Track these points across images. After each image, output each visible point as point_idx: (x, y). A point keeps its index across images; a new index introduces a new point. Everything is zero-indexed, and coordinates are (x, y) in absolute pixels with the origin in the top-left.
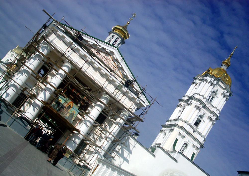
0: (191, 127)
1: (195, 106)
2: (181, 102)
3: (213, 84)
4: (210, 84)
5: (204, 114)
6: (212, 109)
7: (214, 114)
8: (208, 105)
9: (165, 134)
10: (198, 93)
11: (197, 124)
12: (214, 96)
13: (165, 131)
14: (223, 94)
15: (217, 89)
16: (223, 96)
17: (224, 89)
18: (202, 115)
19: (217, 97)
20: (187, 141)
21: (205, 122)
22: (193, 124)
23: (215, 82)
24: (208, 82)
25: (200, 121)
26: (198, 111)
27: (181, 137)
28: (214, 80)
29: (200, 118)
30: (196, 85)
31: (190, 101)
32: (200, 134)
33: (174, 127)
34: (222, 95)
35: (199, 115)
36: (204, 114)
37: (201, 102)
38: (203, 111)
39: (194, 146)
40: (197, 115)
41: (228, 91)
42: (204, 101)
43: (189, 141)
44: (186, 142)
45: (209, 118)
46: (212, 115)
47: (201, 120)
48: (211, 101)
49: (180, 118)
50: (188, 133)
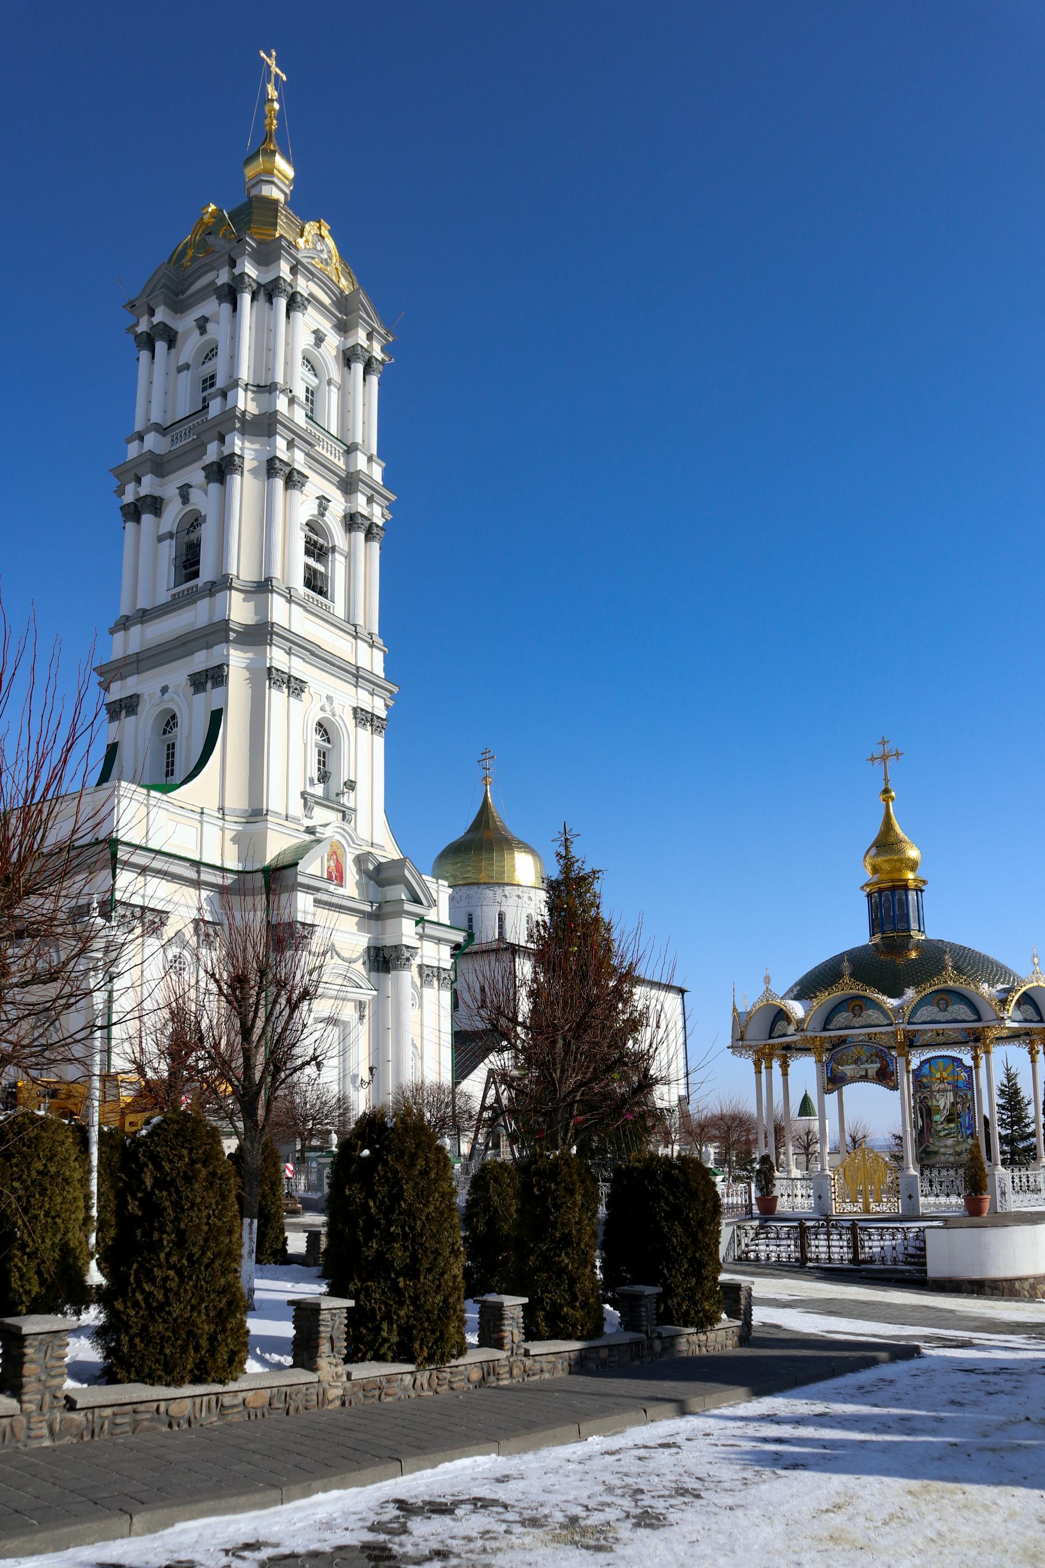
5: (323, 502)
12: (314, 381)
14: (348, 358)
17: (343, 328)
20: (324, 700)
30: (171, 343)
33: (208, 647)
36: (323, 502)
38: (317, 485)
44: (322, 715)
46: (361, 499)
50: (312, 653)
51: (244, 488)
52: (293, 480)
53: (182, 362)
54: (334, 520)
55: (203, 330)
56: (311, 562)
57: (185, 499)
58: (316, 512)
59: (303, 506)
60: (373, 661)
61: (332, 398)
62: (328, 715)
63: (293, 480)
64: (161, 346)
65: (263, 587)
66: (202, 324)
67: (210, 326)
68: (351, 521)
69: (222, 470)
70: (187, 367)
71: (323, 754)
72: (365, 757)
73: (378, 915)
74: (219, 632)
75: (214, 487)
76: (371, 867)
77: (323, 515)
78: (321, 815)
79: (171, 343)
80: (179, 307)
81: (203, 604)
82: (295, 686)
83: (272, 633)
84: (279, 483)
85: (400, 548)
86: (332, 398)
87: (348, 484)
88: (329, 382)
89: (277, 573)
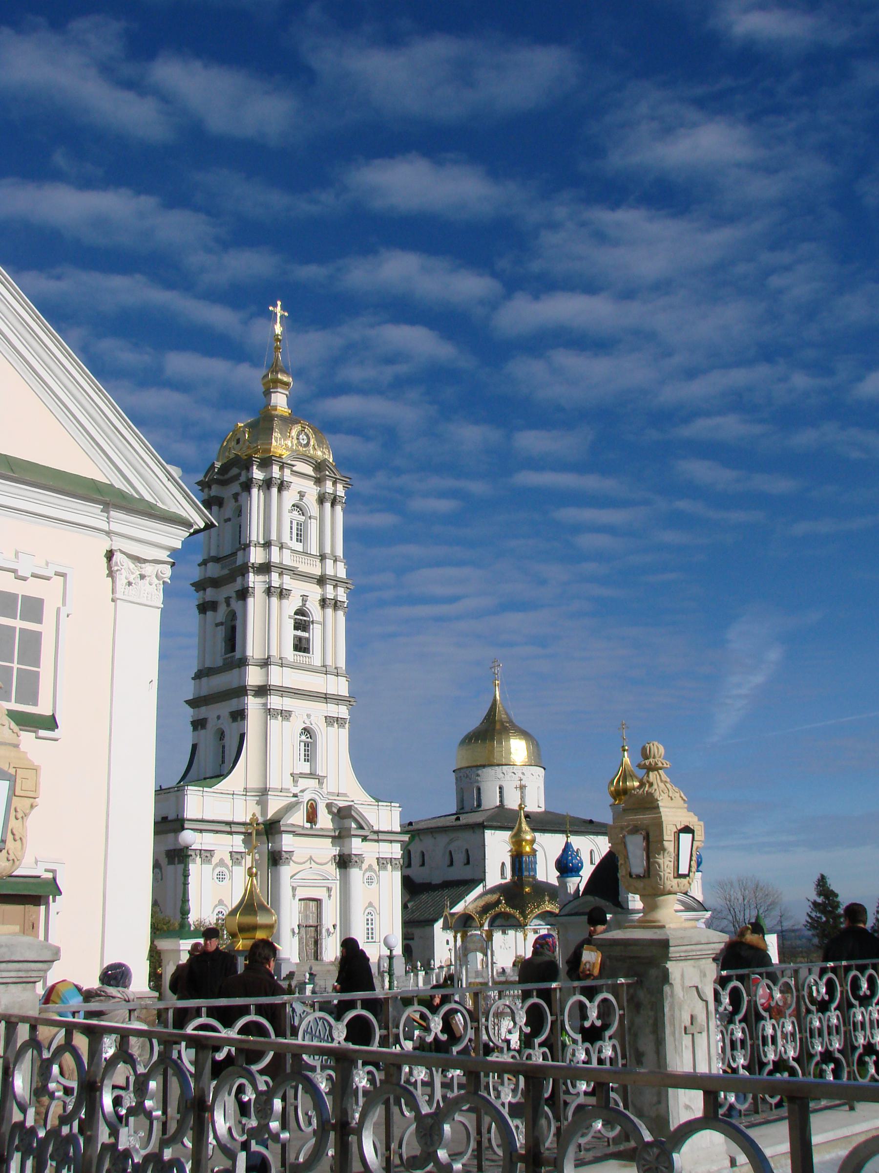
2: (205, 590)
4: (274, 490)
5: (304, 598)
7: (337, 582)
9: (221, 735)
11: (301, 646)
12: (302, 518)
13: (209, 720)
16: (328, 505)
17: (319, 481)
23: (287, 472)
26: (284, 601)
27: (280, 718)
28: (282, 468)
31: (239, 579)
32: (325, 670)
36: (304, 598)
37: (283, 570)
39: (330, 720)
40: (290, 617)
42: (288, 559)
43: (308, 716)
46: (329, 588)
49: (238, 654)
51: (255, 605)
52: (283, 594)
53: (227, 517)
54: (313, 607)
55: (236, 500)
56: (299, 633)
57: (228, 605)
59: (292, 605)
60: (340, 686)
61: (313, 526)
62: (308, 725)
63: (283, 594)
65: (265, 663)
66: (236, 496)
67: (239, 498)
68: (323, 602)
69: (244, 594)
70: (229, 520)
71: (307, 745)
72: (335, 745)
73: (340, 836)
74: (242, 691)
75: (240, 602)
76: (336, 811)
77: (304, 605)
78: (303, 783)
80: (223, 483)
81: (236, 671)
82: (285, 715)
84: (274, 600)
85: (356, 615)
86: (313, 526)
87: (321, 581)
88: (310, 518)
89: (274, 652)
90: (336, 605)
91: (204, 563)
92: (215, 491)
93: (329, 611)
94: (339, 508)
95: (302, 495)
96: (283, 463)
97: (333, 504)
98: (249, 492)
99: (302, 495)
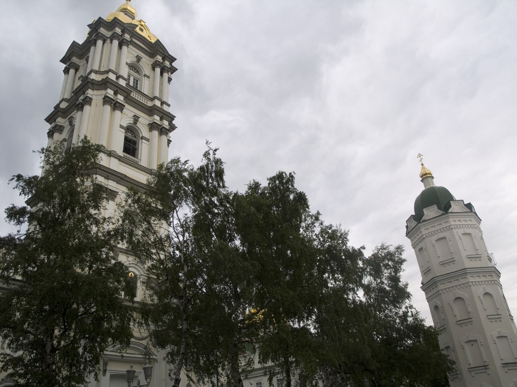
0: (119, 160)
1: (102, 101)
3: (125, 40)
5: (136, 119)
6: (150, 104)
8: (134, 95)
10: (96, 68)
15: (137, 56)
16: (158, 70)
18: (132, 122)
19: (145, 75)
21: (148, 140)
22: (120, 152)
24: (108, 41)
25: (135, 143)
26: (118, 113)
29: (129, 135)
30: (77, 70)
34: (154, 69)
35: (125, 125)
36: (136, 119)
37: (118, 89)
40: (121, 127)
41: (165, 56)
45: (152, 126)
46: (157, 118)
47: (134, 139)
48: (137, 87)
50: (121, 178)
58: (132, 122)
63: (117, 106)
64: (72, 71)
79: (77, 70)
80: (81, 57)
83: (96, 168)
90: (163, 131)
91: (58, 105)
92: (75, 59)
93: (156, 133)
94: (166, 75)
95: (139, 59)
96: (125, 28)
97: (162, 74)
98: (95, 45)
99: (139, 59)
